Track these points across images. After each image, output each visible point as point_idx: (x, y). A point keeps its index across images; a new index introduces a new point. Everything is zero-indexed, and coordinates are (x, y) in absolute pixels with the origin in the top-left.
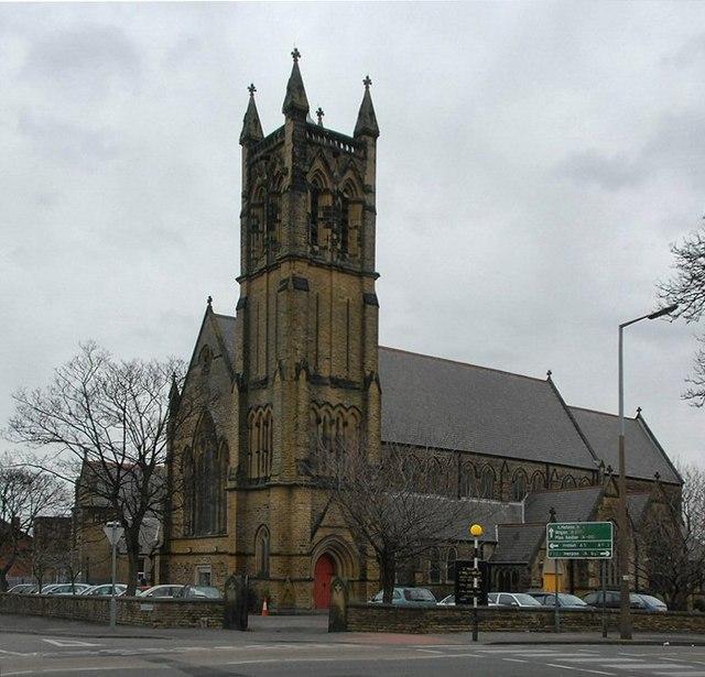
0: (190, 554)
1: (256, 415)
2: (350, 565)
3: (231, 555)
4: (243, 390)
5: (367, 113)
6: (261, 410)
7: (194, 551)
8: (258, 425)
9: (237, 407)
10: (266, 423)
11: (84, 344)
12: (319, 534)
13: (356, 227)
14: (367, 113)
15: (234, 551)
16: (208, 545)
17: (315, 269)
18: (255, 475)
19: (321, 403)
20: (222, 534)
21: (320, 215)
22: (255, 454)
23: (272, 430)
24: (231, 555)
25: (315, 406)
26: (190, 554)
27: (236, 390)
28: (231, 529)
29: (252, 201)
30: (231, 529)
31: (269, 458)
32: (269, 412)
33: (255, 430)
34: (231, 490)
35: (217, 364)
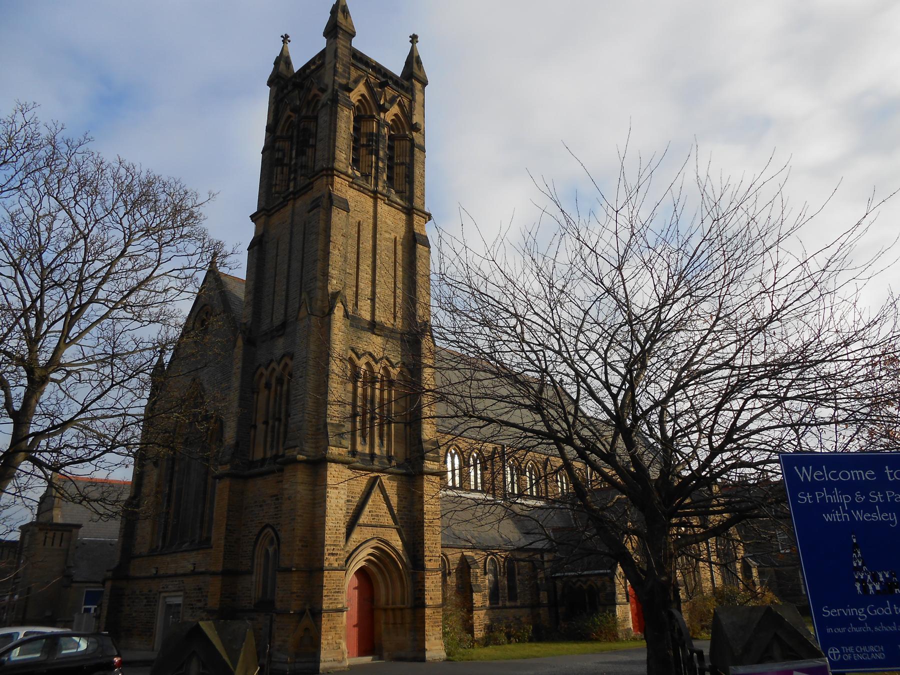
0: (156, 577)
1: (266, 373)
2: (398, 584)
3: (214, 574)
4: (250, 342)
5: (413, 62)
6: (274, 365)
7: (161, 572)
8: (268, 386)
9: (240, 365)
10: (280, 381)
11: (23, 102)
12: (356, 536)
13: (402, 164)
14: (413, 62)
15: (220, 569)
16: (186, 562)
17: (356, 193)
18: (259, 455)
19: (361, 352)
20: (205, 544)
21: (364, 141)
22: (261, 427)
23: (288, 391)
24: (214, 574)
25: (354, 356)
26: (156, 577)
27: (240, 343)
28: (218, 535)
29: (278, 134)
30: (218, 535)
31: (282, 430)
32: (286, 365)
33: (263, 394)
34: (220, 477)
35: (217, 323)
